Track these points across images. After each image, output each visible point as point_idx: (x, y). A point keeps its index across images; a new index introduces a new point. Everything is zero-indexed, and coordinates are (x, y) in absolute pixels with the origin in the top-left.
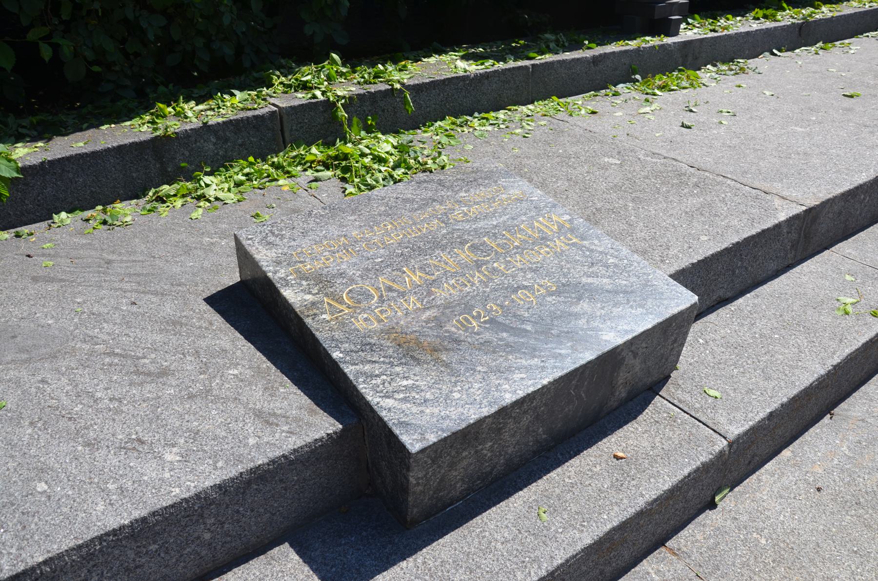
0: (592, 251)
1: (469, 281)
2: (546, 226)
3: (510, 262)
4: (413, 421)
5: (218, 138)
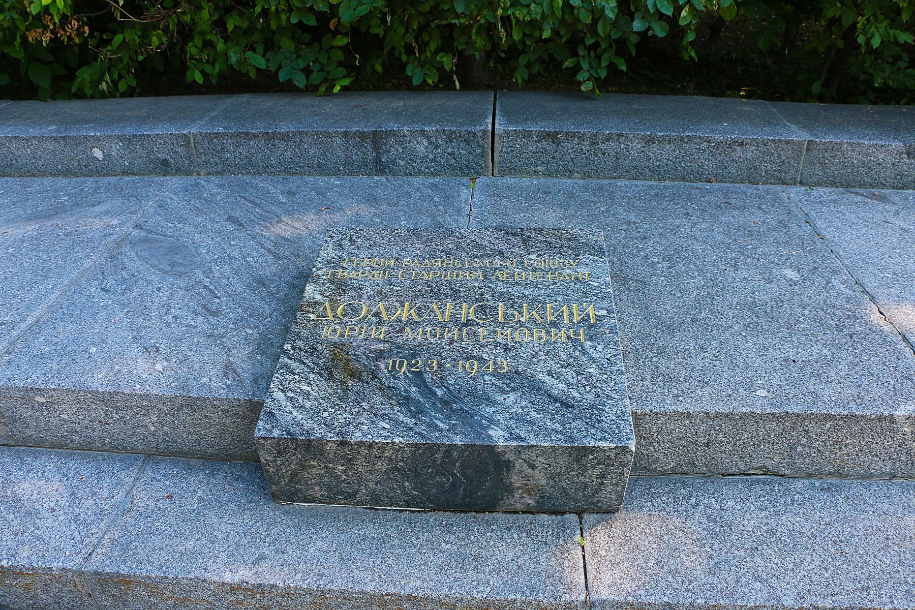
0: (584, 352)
1: (442, 335)
2: (572, 313)
3: (495, 332)
4: (278, 416)
5: (430, 143)
